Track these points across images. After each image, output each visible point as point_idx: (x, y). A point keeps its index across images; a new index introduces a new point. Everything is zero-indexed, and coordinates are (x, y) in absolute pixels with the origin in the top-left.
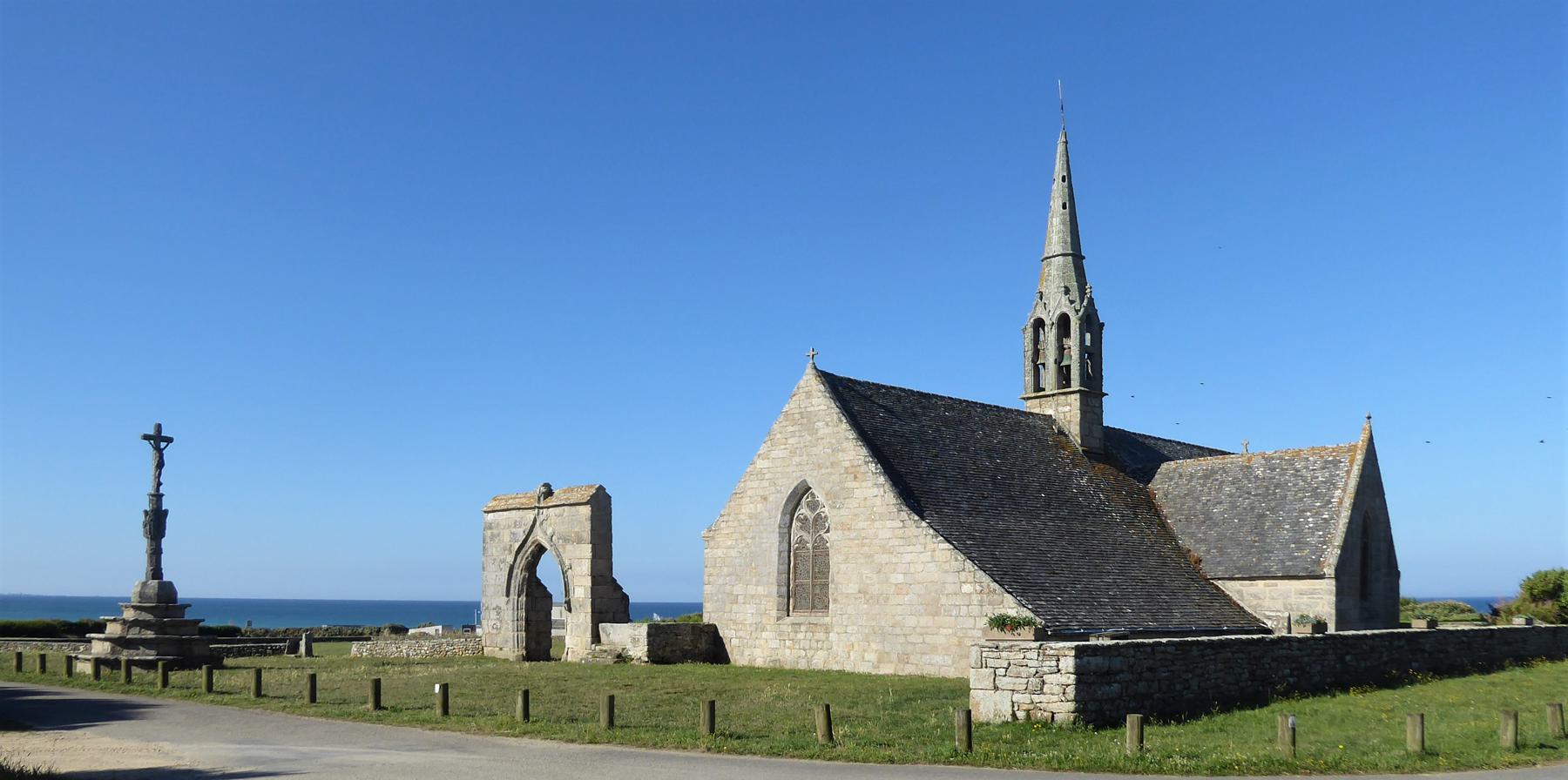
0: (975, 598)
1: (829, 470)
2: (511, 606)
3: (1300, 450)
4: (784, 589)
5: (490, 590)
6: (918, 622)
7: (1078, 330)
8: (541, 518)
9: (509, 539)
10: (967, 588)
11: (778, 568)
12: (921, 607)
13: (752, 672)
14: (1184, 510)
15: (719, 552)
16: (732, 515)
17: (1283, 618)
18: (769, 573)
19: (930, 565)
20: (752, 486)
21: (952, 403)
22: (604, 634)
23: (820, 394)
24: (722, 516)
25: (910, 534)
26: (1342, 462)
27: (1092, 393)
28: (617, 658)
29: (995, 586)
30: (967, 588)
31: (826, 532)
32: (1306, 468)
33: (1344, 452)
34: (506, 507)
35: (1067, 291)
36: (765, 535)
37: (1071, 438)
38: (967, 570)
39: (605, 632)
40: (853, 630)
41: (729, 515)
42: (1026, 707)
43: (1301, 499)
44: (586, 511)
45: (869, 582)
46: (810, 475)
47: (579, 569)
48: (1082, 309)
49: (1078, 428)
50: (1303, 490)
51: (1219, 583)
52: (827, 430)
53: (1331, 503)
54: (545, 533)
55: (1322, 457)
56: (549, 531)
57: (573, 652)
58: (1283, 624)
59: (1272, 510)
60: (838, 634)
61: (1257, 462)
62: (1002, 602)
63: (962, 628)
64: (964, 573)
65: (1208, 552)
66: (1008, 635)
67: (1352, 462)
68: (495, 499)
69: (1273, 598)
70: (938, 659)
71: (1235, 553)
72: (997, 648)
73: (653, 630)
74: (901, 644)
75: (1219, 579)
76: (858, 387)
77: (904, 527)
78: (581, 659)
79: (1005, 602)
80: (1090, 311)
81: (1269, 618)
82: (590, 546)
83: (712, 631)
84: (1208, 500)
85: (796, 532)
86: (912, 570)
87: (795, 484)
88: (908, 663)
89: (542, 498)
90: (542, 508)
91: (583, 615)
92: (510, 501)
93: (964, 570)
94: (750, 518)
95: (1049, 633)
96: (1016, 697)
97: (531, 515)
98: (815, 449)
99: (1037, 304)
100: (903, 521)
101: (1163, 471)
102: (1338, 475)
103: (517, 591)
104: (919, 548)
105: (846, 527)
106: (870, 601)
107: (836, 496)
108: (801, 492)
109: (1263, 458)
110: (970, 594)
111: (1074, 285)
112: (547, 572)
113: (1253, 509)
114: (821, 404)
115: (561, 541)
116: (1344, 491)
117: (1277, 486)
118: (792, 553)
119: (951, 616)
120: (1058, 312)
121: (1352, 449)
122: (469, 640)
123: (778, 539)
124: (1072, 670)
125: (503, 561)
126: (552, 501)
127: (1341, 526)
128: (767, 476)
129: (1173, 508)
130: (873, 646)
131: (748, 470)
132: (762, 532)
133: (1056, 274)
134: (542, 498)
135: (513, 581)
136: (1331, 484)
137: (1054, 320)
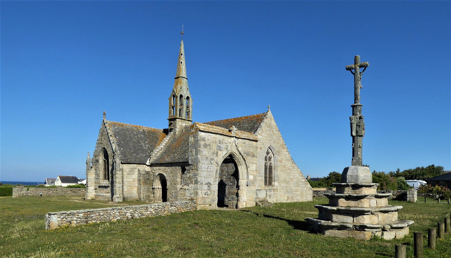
1: (277, 144)
9: (216, 149)
10: (303, 180)
104: (295, 170)
120: (187, 96)
128: (261, 141)
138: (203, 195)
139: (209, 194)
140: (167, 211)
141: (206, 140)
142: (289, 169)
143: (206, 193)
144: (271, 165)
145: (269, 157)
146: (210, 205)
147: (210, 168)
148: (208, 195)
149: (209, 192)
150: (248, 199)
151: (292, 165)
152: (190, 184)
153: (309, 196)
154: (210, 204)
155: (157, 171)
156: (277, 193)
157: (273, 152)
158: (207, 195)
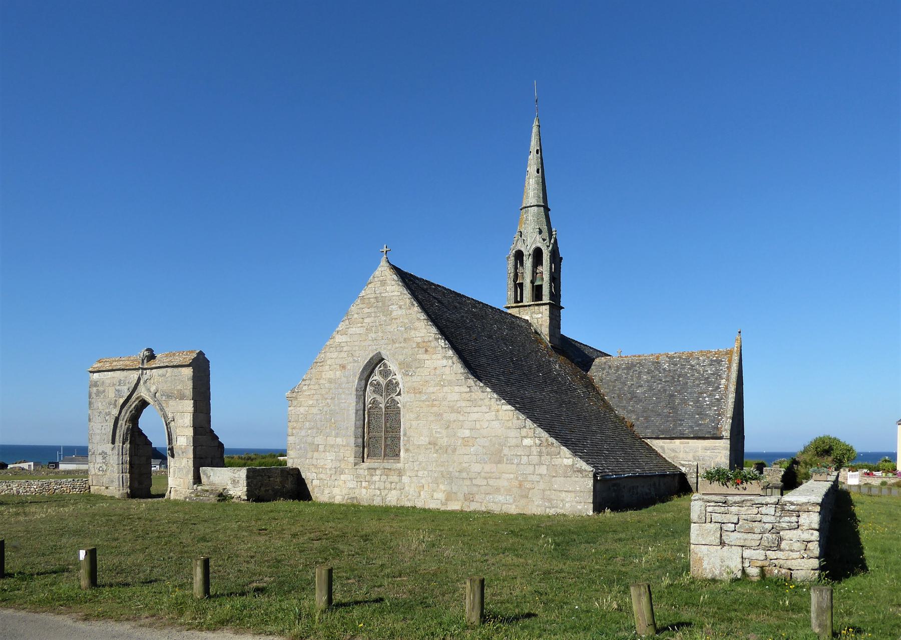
0: (535, 450)
1: (402, 345)
2: (116, 452)
3: (693, 353)
4: (360, 440)
5: (97, 439)
6: (483, 468)
7: (549, 260)
8: (145, 377)
10: (527, 442)
11: (355, 424)
12: (485, 457)
13: (331, 508)
14: (615, 390)
15: (302, 410)
16: (314, 380)
17: (694, 466)
18: (347, 428)
19: (494, 423)
20: (331, 357)
21: (475, 303)
22: (205, 477)
23: (393, 283)
24: (304, 380)
25: (476, 397)
26: (723, 361)
27: (555, 308)
28: (219, 496)
29: (552, 440)
30: (527, 442)
31: (396, 396)
32: (699, 364)
33: (723, 355)
34: (110, 368)
35: (540, 232)
36: (343, 396)
37: (543, 336)
38: (527, 427)
39: (205, 474)
40: (423, 474)
41: (310, 380)
42: (760, 564)
43: (698, 385)
44: (188, 372)
45: (438, 435)
46: (384, 349)
47: (181, 421)
48: (551, 246)
49: (548, 329)
50: (699, 379)
51: (648, 441)
52: (400, 312)
53: (720, 388)
54: (149, 390)
55: (709, 357)
56: (153, 389)
57: (176, 491)
58: (693, 470)
59: (679, 392)
60: (410, 477)
61: (663, 359)
62: (559, 453)
63: (523, 474)
64: (525, 430)
65: (637, 419)
66: (732, 490)
67: (730, 361)
68: (99, 362)
69: (686, 452)
70: (500, 498)
71: (657, 420)
72: (725, 503)
73: (251, 473)
74: (467, 486)
75: (649, 438)
76: (417, 281)
77: (470, 391)
78: (186, 498)
79: (561, 453)
80: (555, 248)
81: (683, 465)
82: (192, 401)
83: (296, 473)
84: (632, 384)
85: (370, 395)
86: (478, 426)
87: (371, 356)
88: (473, 501)
89: (145, 361)
90: (146, 369)
91: (184, 461)
92: (115, 363)
93: (525, 427)
94: (331, 383)
95: (599, 478)
96: (747, 553)
97: (135, 375)
98: (389, 327)
99: (518, 240)
100: (470, 387)
101: (597, 363)
102: (722, 370)
103: (121, 439)
104: (484, 409)
105: (417, 391)
106: (440, 451)
107: (409, 366)
108: (375, 362)
109: (667, 356)
110: (531, 446)
111: (545, 228)
112: (148, 423)
113: (665, 391)
114: (395, 290)
115: (164, 397)
116: (728, 380)
117: (679, 376)
118: (366, 412)
119: (513, 463)
121: (729, 353)
122: (76, 480)
123: (355, 400)
124: (817, 526)
125: (109, 414)
126: (153, 364)
127: (730, 404)
128: (345, 349)
129: (608, 389)
130: (442, 487)
131: (328, 343)
132: (341, 394)
133: (530, 222)
134: (145, 361)
135: (118, 431)
136: (717, 375)
137: (531, 252)
138: (97, 471)
139: (105, 470)
142: (453, 410)
143: (101, 469)
146: (107, 488)
149: (105, 467)
150: (177, 483)
151: (467, 396)
153: (569, 497)
154: (107, 486)
156: (400, 481)
158: (101, 471)
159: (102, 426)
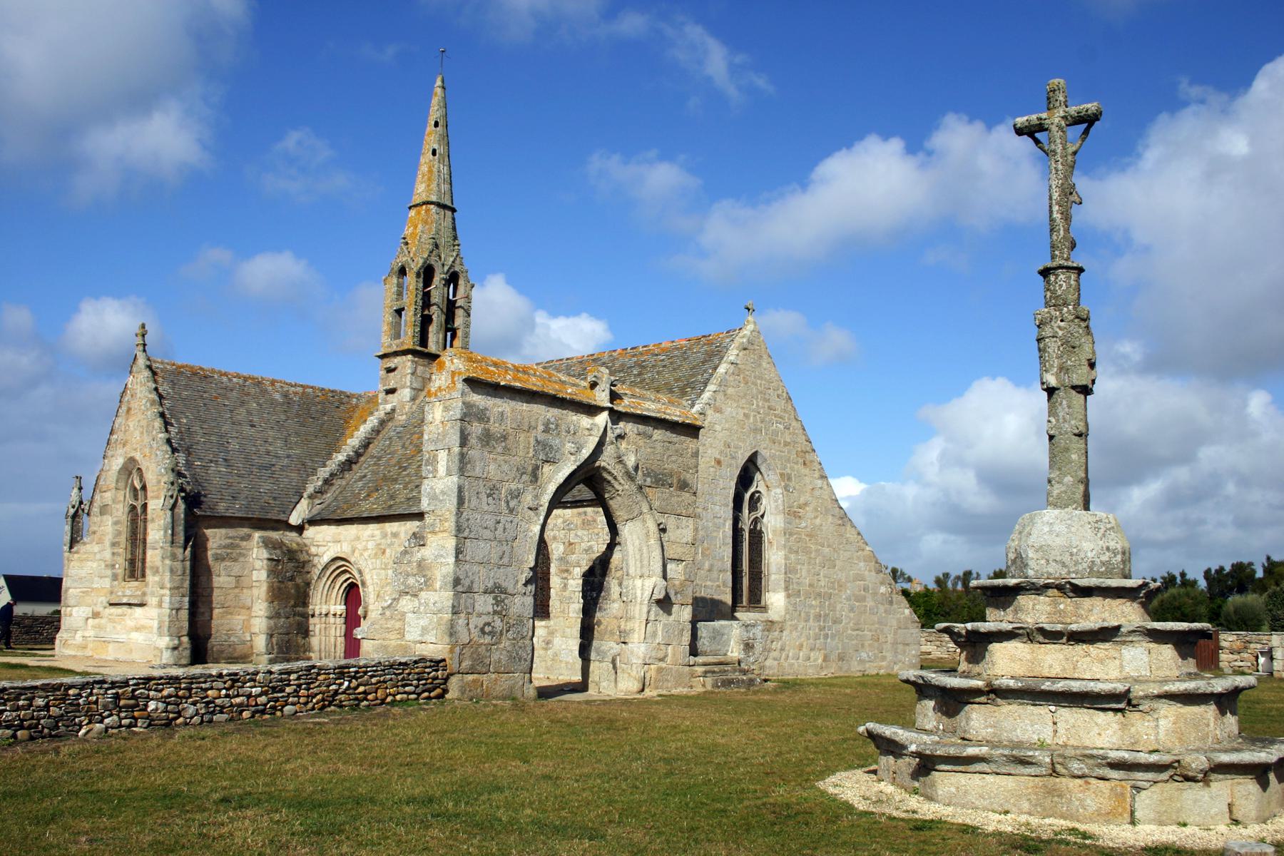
138: (475, 633)
140: (319, 697)
141: (489, 419)
144: (758, 528)
145: (753, 495)
147: (505, 529)
148: (492, 633)
149: (498, 624)
152: (421, 590)
155: (325, 548)
157: (766, 476)
159: (499, 522)
